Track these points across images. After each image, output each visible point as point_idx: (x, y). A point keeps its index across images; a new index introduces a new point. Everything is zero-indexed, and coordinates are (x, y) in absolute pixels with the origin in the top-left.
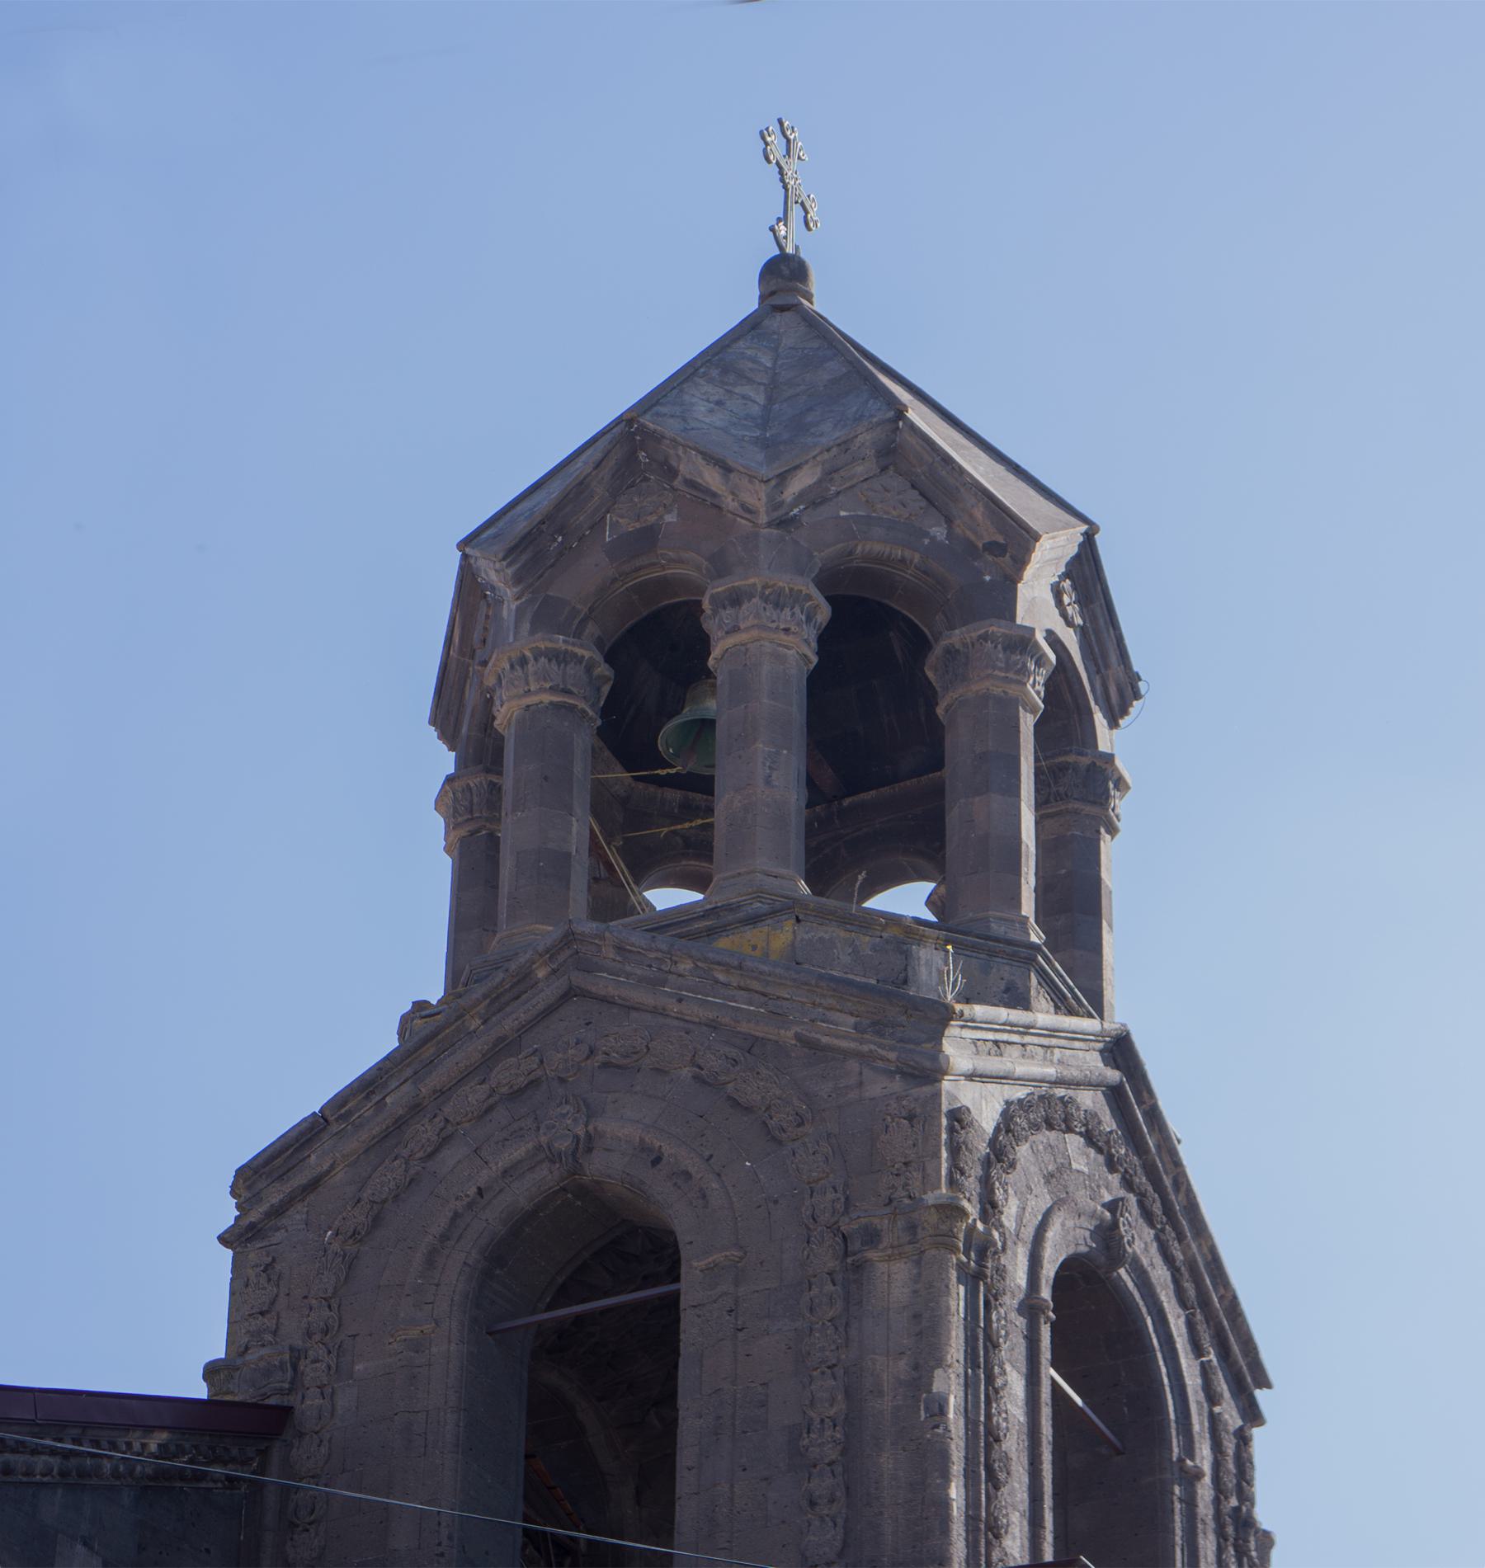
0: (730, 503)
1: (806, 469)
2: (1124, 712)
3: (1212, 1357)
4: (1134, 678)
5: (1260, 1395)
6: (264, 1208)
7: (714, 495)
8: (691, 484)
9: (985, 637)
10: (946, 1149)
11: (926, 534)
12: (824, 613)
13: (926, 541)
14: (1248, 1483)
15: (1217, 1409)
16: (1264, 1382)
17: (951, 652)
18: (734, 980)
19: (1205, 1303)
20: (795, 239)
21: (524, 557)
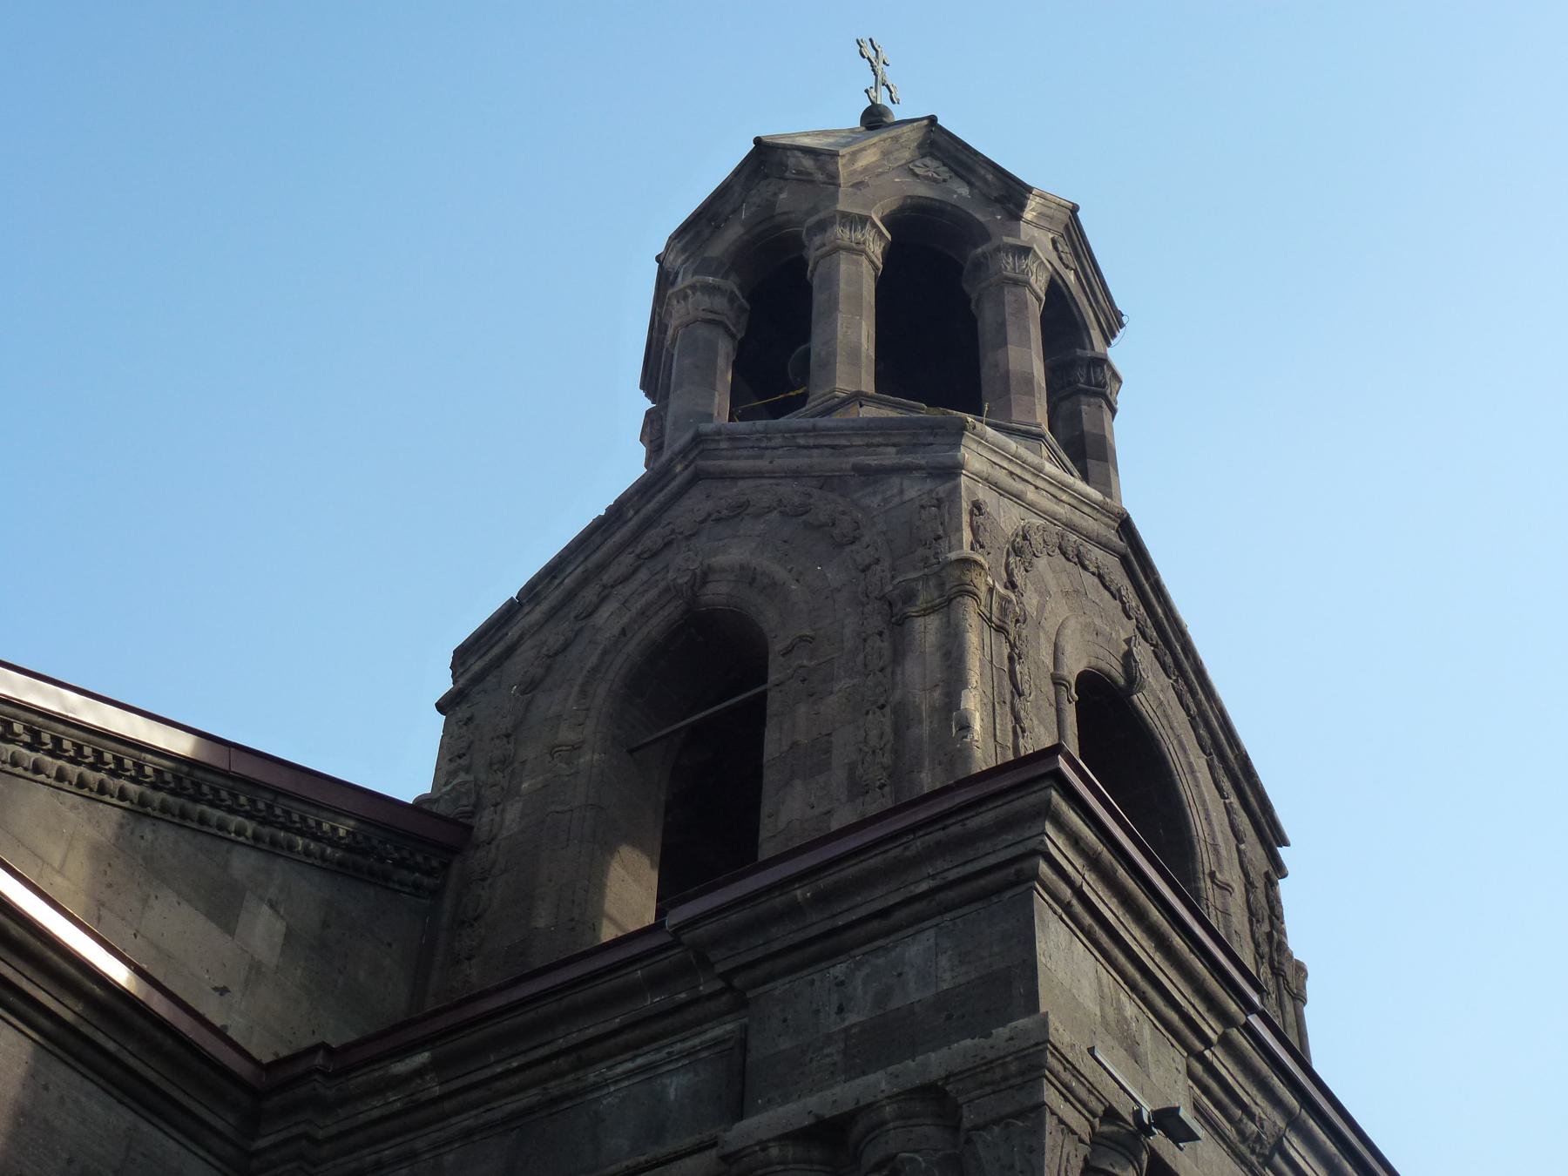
1: (871, 151)
2: (1114, 336)
3: (1234, 800)
4: (1119, 315)
5: (1282, 851)
6: (468, 675)
7: (811, 174)
10: (1113, 1132)
11: (955, 192)
13: (955, 196)
14: (1278, 919)
15: (1242, 847)
16: (1284, 842)
18: (811, 442)
19: (1223, 758)
20: (883, 99)
21: (687, 238)
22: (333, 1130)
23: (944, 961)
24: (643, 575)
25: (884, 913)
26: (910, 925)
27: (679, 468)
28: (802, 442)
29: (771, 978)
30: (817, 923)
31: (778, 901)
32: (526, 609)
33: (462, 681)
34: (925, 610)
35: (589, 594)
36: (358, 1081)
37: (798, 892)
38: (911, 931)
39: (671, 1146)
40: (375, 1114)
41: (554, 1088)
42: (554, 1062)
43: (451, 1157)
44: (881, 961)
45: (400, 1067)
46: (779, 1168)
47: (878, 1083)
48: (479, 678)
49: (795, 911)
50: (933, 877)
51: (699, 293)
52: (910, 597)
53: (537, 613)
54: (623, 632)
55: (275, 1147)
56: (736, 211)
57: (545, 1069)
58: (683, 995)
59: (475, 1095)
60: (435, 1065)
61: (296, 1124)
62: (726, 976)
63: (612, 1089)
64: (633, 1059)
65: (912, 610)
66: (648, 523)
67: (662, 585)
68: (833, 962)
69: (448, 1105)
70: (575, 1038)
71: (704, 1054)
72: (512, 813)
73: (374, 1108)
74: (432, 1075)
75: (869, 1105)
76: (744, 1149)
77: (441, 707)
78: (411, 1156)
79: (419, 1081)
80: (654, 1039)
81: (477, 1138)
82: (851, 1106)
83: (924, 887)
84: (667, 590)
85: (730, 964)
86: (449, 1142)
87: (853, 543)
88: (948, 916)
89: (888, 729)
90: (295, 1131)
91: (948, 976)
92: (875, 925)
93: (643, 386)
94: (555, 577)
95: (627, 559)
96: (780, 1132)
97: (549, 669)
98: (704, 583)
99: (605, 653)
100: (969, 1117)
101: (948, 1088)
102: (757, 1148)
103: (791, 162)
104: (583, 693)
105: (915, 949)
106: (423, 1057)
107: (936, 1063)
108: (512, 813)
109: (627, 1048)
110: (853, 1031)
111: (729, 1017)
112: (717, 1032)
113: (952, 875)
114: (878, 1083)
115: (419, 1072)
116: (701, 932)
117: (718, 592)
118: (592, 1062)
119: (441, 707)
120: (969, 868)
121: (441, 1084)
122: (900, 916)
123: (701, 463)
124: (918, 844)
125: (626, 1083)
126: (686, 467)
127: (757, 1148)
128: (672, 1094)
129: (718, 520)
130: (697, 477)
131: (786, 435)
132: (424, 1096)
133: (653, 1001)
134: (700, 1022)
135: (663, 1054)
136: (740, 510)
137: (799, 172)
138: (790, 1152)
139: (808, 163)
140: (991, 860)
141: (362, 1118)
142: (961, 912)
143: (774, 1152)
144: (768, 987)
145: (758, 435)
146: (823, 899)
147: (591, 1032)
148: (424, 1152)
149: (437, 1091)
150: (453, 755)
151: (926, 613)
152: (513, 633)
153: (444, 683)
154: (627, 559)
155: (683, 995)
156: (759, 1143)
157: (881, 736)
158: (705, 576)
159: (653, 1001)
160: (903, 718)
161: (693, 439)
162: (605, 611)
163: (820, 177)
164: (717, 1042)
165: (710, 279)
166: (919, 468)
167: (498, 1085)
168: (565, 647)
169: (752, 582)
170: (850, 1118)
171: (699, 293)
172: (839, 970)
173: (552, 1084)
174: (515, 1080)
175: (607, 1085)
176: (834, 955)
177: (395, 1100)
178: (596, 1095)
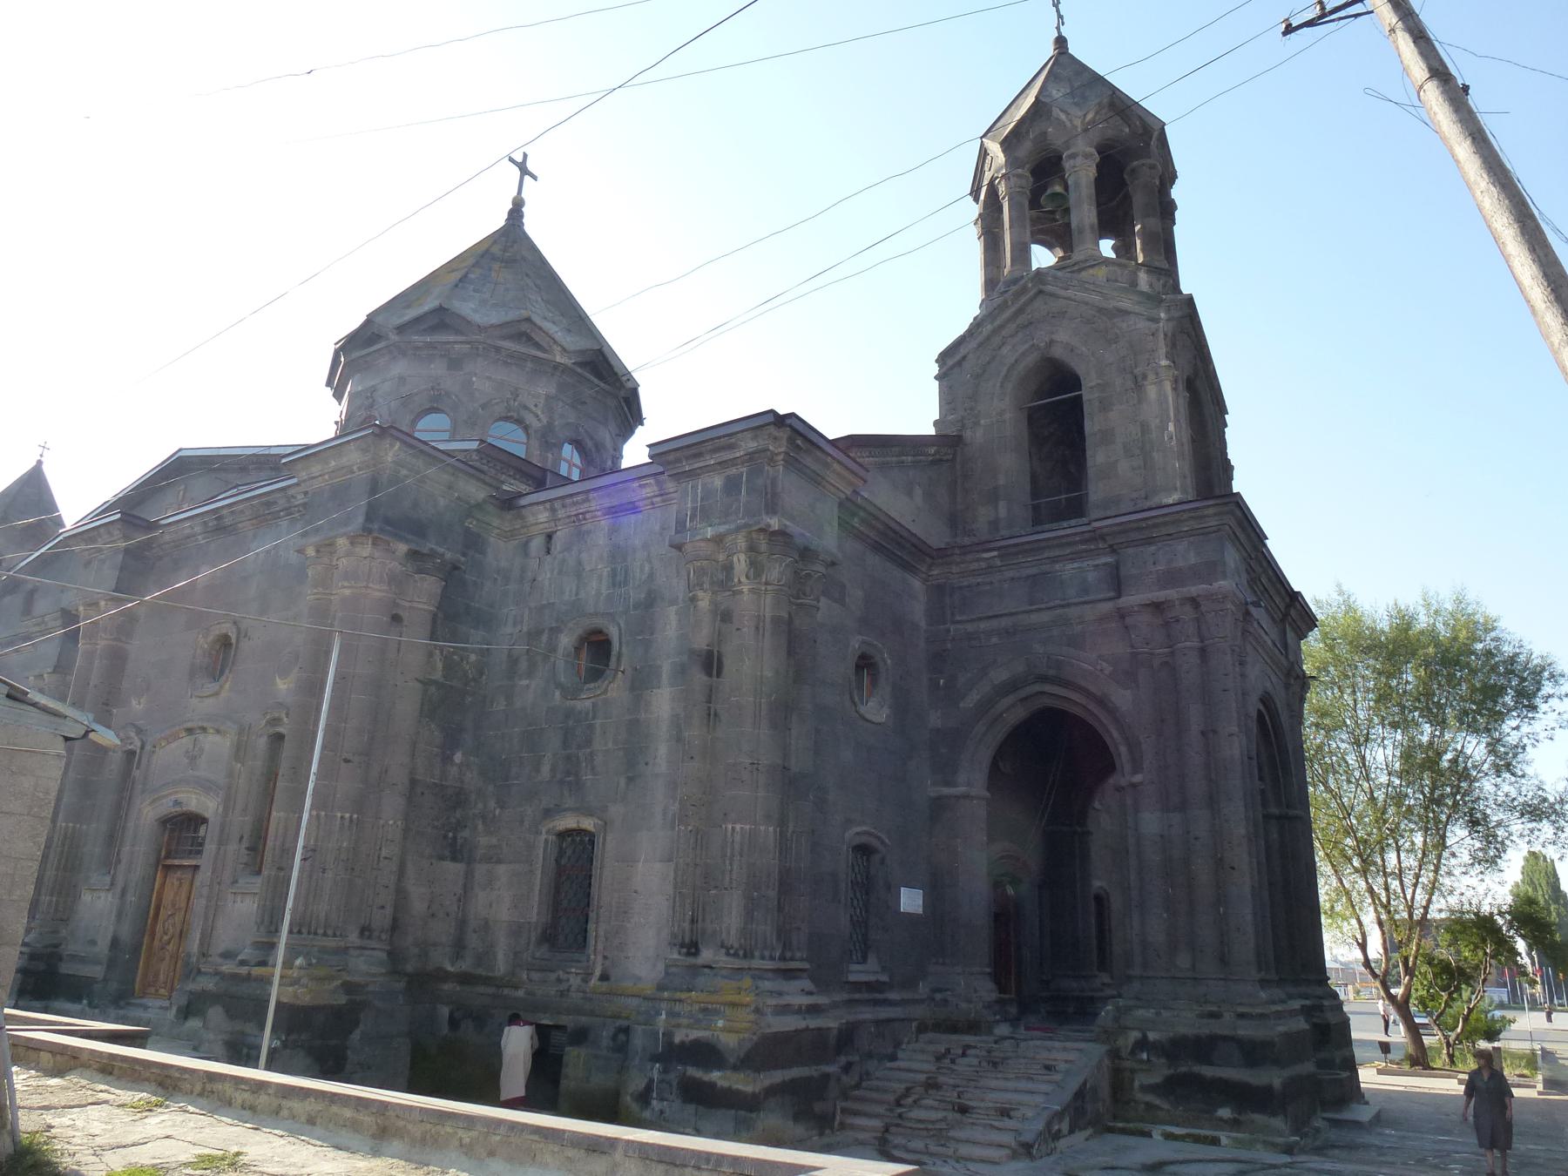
0: (1068, 124)
8: (1057, 119)
9: (1143, 165)
12: (1097, 157)
17: (1133, 171)
23: (1192, 554)
24: (1020, 335)
33: (944, 369)
35: (997, 340)
39: (1092, 597)
45: (986, 555)
47: (1172, 594)
48: (952, 368)
52: (1145, 377)
53: (973, 344)
54: (1016, 361)
56: (1028, 132)
60: (999, 556)
62: (1111, 546)
65: (1145, 383)
66: (1021, 311)
67: (1031, 343)
72: (980, 433)
73: (975, 566)
77: (936, 378)
84: (1033, 345)
91: (1193, 559)
95: (1012, 327)
97: (984, 371)
99: (1008, 371)
100: (1203, 608)
104: (1002, 386)
105: (1181, 546)
106: (995, 553)
107: (1194, 590)
108: (980, 433)
114: (1172, 594)
116: (1105, 530)
117: (1058, 352)
119: (936, 378)
122: (1175, 535)
123: (1041, 287)
124: (1185, 516)
128: (1090, 579)
136: (1062, 314)
150: (948, 399)
151: (1152, 384)
152: (963, 351)
153: (935, 369)
154: (1012, 327)
158: (1052, 342)
160: (1145, 428)
162: (1005, 350)
167: (1023, 565)
168: (989, 363)
169: (1072, 350)
170: (1163, 603)
172: (1153, 548)
176: (1150, 544)
177: (983, 565)
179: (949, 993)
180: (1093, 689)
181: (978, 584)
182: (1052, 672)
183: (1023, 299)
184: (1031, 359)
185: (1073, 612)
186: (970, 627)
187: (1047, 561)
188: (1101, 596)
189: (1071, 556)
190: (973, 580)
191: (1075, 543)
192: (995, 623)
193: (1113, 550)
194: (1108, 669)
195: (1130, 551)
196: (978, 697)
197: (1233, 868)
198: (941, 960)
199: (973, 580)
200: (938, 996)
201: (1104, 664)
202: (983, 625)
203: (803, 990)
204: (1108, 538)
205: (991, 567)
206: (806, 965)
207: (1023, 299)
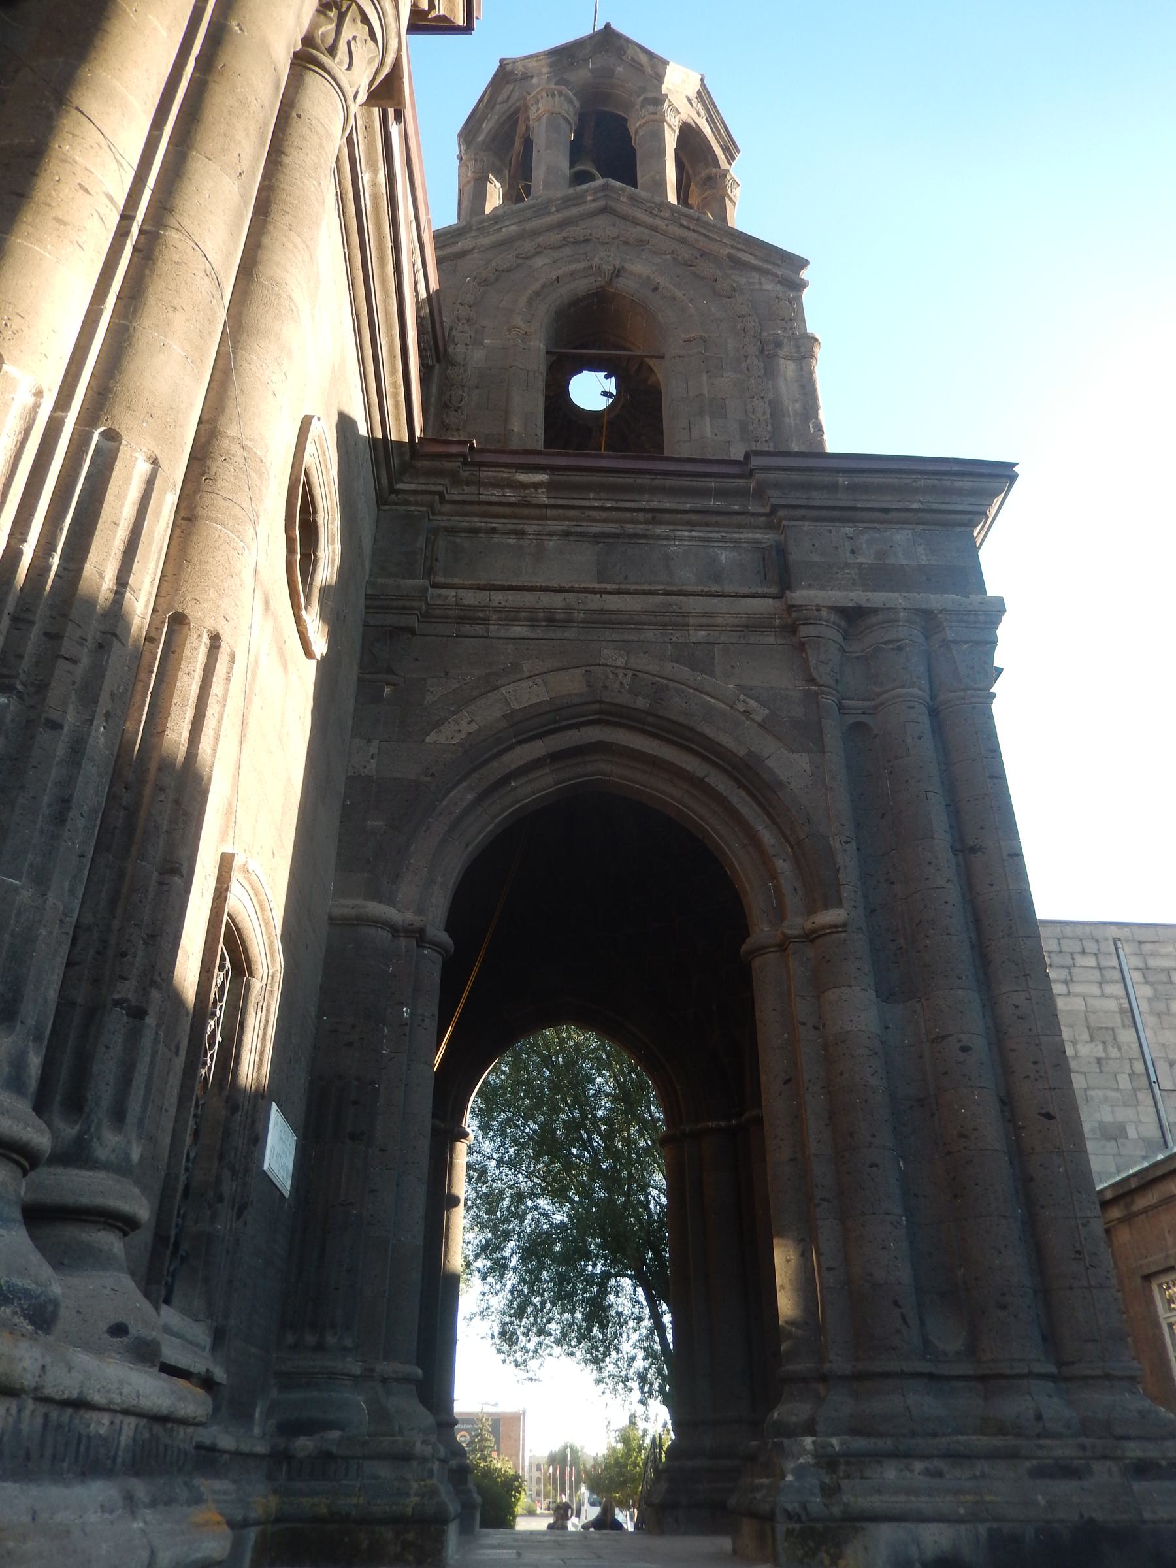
22: (458, 498)
25: (886, 510)
26: (898, 523)
27: (589, 198)
28: (685, 223)
29: (803, 518)
30: (844, 500)
31: (827, 479)
32: (474, 234)
34: (787, 356)
36: (486, 474)
37: (840, 479)
38: (896, 526)
40: (493, 499)
41: (630, 528)
42: (635, 514)
43: (551, 543)
44: (877, 535)
46: (824, 623)
49: (833, 488)
50: (922, 503)
51: (562, 98)
52: (778, 345)
55: (415, 492)
56: (586, 61)
57: (628, 515)
58: (736, 507)
59: (571, 513)
60: (550, 486)
61: (435, 484)
62: (775, 509)
63: (677, 543)
64: (690, 531)
67: (587, 264)
68: (844, 525)
69: (549, 512)
70: (654, 504)
71: (745, 545)
73: (494, 495)
74: (544, 490)
75: (889, 608)
76: (806, 606)
78: (521, 533)
79: (533, 490)
80: (707, 525)
81: (571, 538)
82: (881, 605)
83: (915, 506)
84: (591, 267)
85: (782, 502)
86: (550, 534)
87: (729, 297)
88: (921, 527)
89: (769, 411)
90: (433, 488)
92: (877, 515)
93: (460, 135)
94: (496, 223)
96: (830, 604)
97: (497, 280)
98: (618, 276)
99: (544, 286)
101: (940, 616)
102: (814, 608)
103: (630, 52)
104: (530, 302)
106: (544, 477)
109: (688, 523)
110: (864, 566)
111: (761, 531)
112: (758, 536)
113: (935, 506)
115: (536, 486)
116: (772, 476)
117: (626, 285)
118: (661, 523)
120: (944, 507)
121: (548, 498)
125: (687, 543)
126: (594, 200)
127: (814, 608)
129: (626, 243)
130: (604, 210)
131: (675, 214)
132: (535, 501)
133: (713, 503)
134: (740, 526)
135: (719, 535)
137: (633, 60)
138: (833, 617)
139: (643, 59)
140: (960, 508)
141: (483, 498)
142: (930, 527)
143: (824, 613)
144: (801, 523)
145: (653, 205)
146: (852, 488)
147: (668, 506)
148: (530, 534)
149: (546, 501)
151: (787, 358)
154: (555, 237)
155: (736, 507)
156: (818, 605)
157: (764, 413)
159: (713, 503)
161: (603, 185)
162: (539, 262)
163: (649, 70)
164: (756, 542)
165: (570, 93)
166: (776, 275)
170: (875, 611)
171: (562, 98)
173: (628, 526)
174: (605, 515)
175: (674, 540)
177: (511, 496)
178: (664, 542)
179: (335, 1434)
180: (726, 740)
181: (494, 530)
182: (641, 703)
183: (574, 211)
184: (583, 286)
185: (690, 603)
186: (469, 598)
187: (641, 516)
188: (746, 590)
189: (693, 517)
190: (478, 522)
191: (705, 493)
192: (528, 599)
193: (772, 521)
194: (761, 713)
195: (807, 526)
196: (474, 727)
197: (1049, 1116)
198: (310, 1339)
199: (478, 522)
200: (304, 1445)
201: (752, 702)
202: (498, 598)
203: (119, 1330)
204: (770, 492)
205: (529, 505)
206: (141, 1209)
207: (574, 211)
